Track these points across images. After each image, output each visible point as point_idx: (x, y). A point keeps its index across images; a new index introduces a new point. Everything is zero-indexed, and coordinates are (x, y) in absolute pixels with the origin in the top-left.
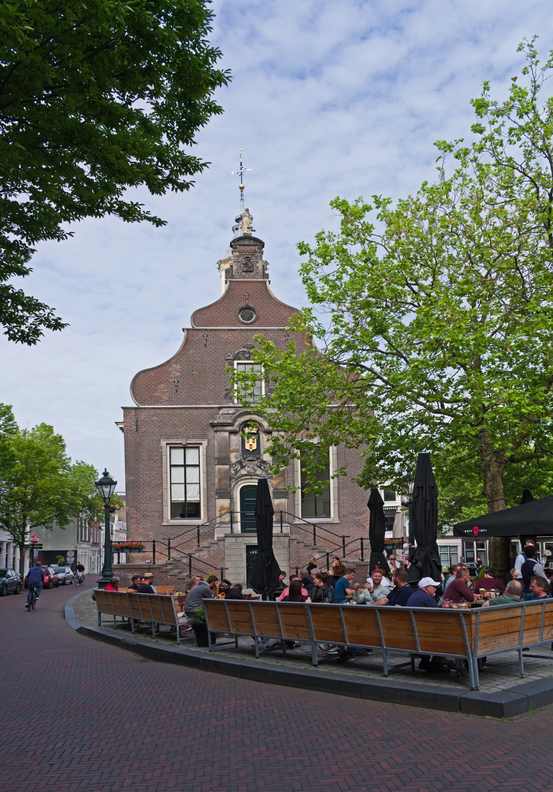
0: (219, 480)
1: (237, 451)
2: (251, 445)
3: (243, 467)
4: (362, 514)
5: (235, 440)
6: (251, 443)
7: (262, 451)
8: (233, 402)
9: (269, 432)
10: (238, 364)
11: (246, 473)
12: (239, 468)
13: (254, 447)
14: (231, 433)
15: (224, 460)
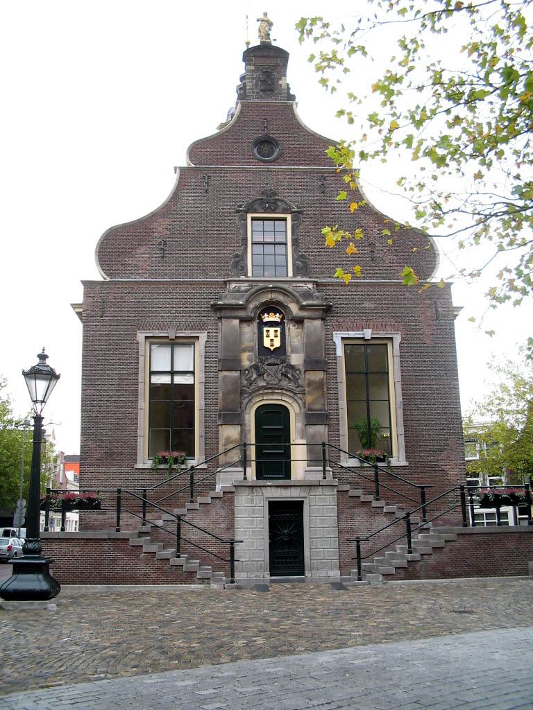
0: (223, 394)
1: (251, 349)
2: (272, 340)
3: (260, 375)
4: (441, 452)
5: (249, 331)
6: (272, 336)
7: (289, 349)
8: (246, 275)
9: (299, 321)
10: (253, 219)
11: (264, 384)
12: (255, 376)
13: (277, 343)
14: (243, 320)
15: (230, 363)
